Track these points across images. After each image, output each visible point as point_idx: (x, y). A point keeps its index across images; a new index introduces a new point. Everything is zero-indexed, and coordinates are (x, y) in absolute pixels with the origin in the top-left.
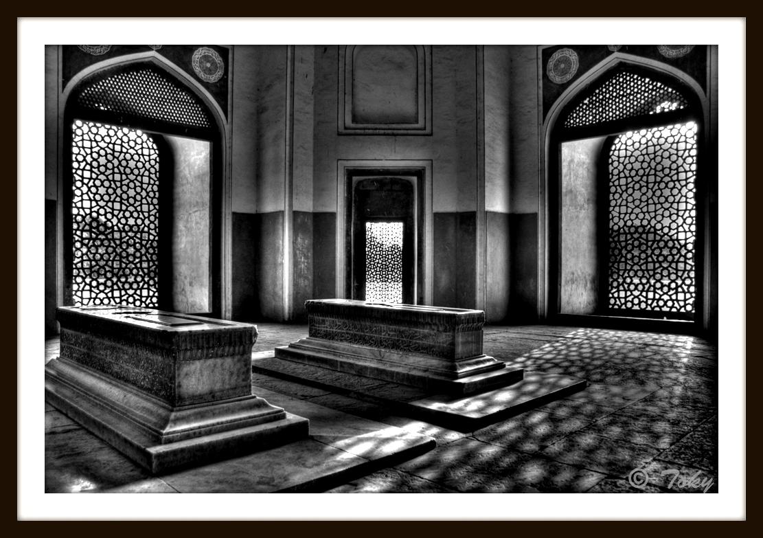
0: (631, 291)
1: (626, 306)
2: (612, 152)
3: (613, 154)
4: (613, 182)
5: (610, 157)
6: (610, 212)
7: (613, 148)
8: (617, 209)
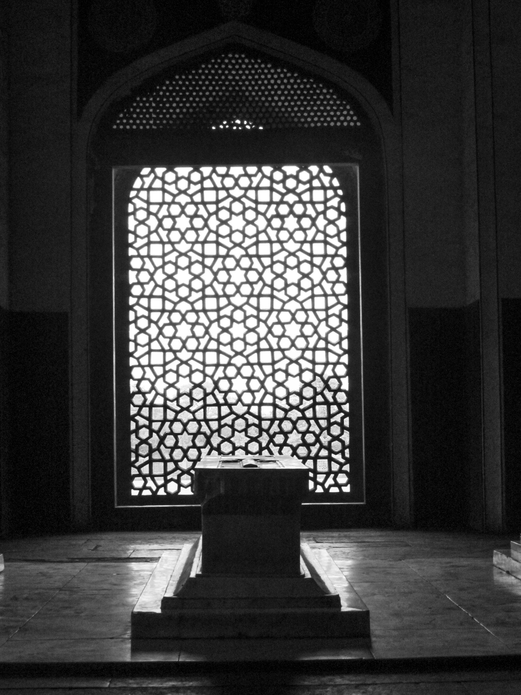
0: (176, 462)
1: (166, 490)
2: (133, 194)
3: (137, 196)
4: (137, 250)
5: (130, 200)
6: (131, 308)
7: (137, 183)
8: (144, 302)
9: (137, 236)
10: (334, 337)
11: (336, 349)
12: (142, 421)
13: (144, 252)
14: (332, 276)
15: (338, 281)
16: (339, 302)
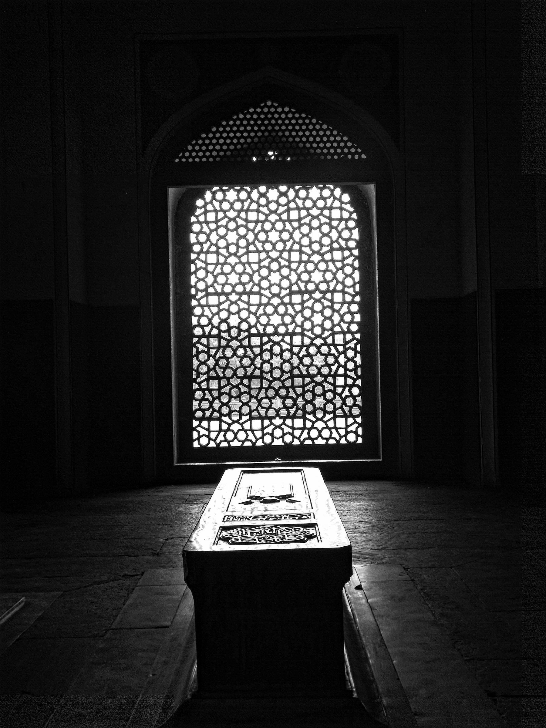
9: (198, 290)
10: (350, 365)
11: (352, 374)
12: (203, 432)
13: (203, 302)
14: (348, 318)
15: (352, 322)
16: (354, 338)
